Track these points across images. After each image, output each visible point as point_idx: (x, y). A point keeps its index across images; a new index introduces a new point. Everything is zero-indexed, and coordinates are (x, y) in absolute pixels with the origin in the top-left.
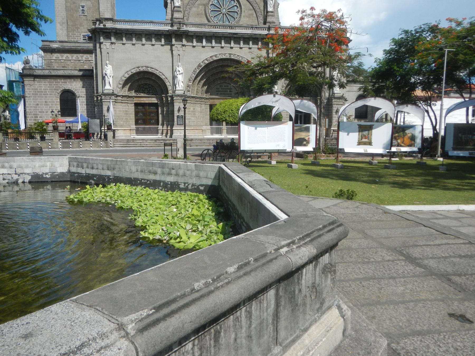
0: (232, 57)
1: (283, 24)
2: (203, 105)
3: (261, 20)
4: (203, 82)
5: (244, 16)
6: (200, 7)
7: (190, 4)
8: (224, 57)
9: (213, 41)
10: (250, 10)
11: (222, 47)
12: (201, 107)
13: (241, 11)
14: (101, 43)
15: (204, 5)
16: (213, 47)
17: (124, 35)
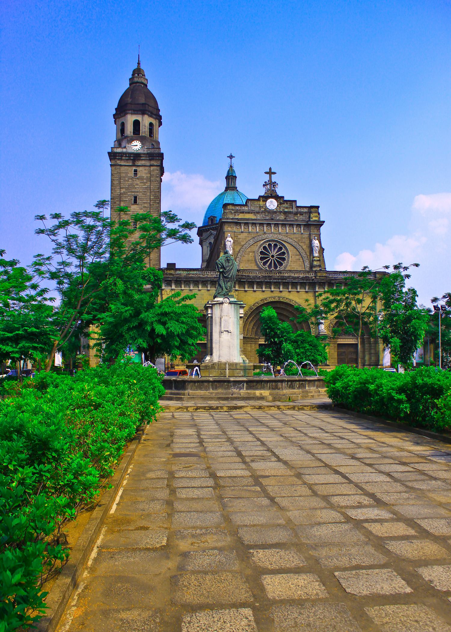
0: (281, 300)
1: (327, 270)
2: (253, 345)
3: (307, 264)
4: (253, 323)
5: (291, 261)
6: (251, 254)
7: (241, 252)
8: (274, 300)
9: (264, 287)
10: (297, 255)
11: (272, 291)
12: (251, 347)
13: (289, 257)
14: (162, 290)
15: (254, 252)
16: (263, 291)
17: (183, 282)
